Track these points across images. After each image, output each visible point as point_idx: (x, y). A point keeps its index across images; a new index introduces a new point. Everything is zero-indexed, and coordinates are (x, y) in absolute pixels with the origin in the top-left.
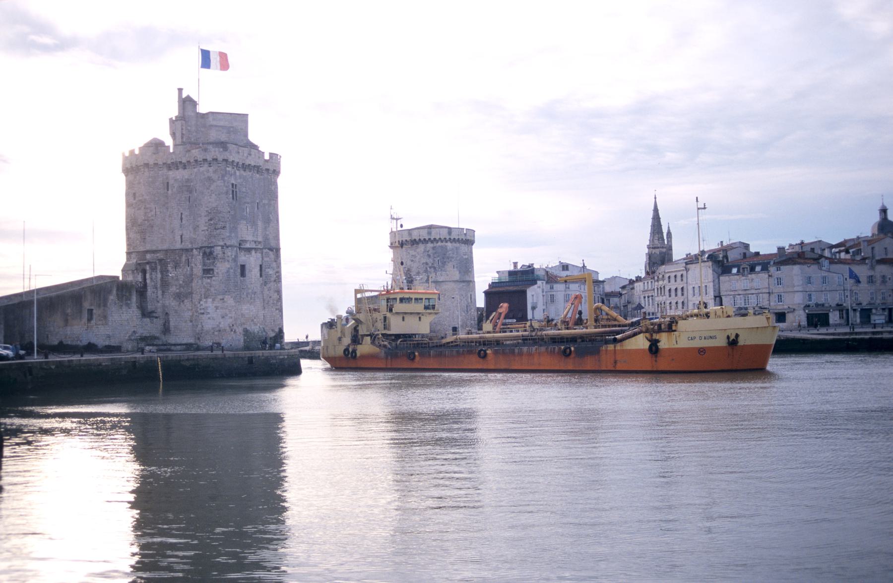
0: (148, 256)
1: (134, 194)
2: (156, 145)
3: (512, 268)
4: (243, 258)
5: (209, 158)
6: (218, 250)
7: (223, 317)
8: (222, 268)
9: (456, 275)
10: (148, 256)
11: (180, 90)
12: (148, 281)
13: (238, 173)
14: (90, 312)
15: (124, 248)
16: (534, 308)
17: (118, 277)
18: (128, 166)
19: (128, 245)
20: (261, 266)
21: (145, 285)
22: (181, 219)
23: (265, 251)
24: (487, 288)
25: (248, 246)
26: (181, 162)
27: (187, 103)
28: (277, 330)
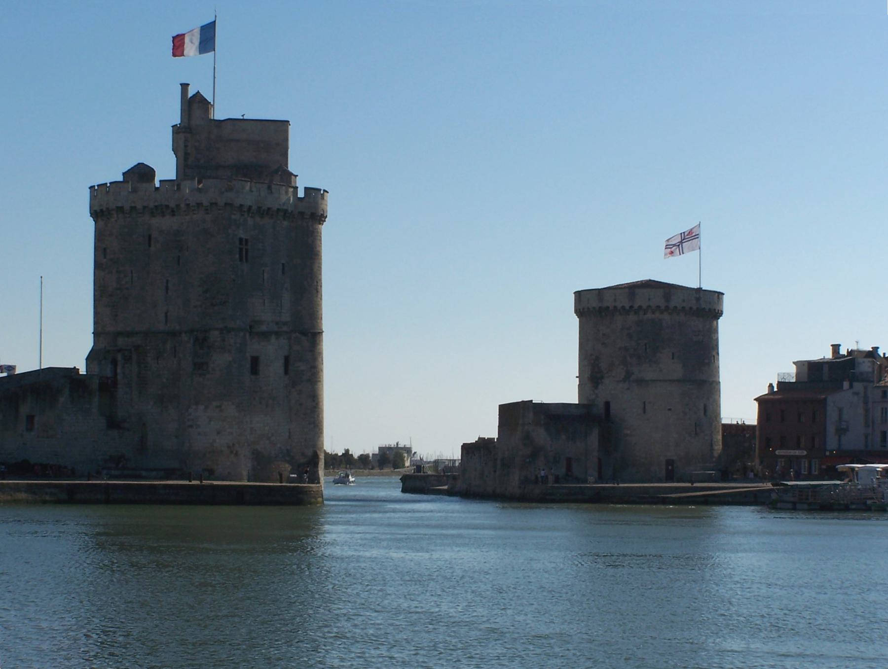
0: (121, 341)
1: (105, 250)
2: (141, 173)
3: (829, 355)
4: (255, 347)
5: (206, 203)
6: (214, 335)
7: (218, 433)
8: (219, 360)
9: (677, 370)
10: (121, 341)
11: (185, 86)
12: (119, 377)
13: (250, 221)
14: (30, 419)
15: (90, 327)
16: (841, 431)
17: (75, 370)
18: (96, 208)
19: (95, 323)
20: (287, 360)
21: (115, 384)
22: (167, 289)
23: (294, 335)
24: (765, 391)
25: (264, 328)
26: (167, 207)
27: (194, 105)
28: (310, 453)
